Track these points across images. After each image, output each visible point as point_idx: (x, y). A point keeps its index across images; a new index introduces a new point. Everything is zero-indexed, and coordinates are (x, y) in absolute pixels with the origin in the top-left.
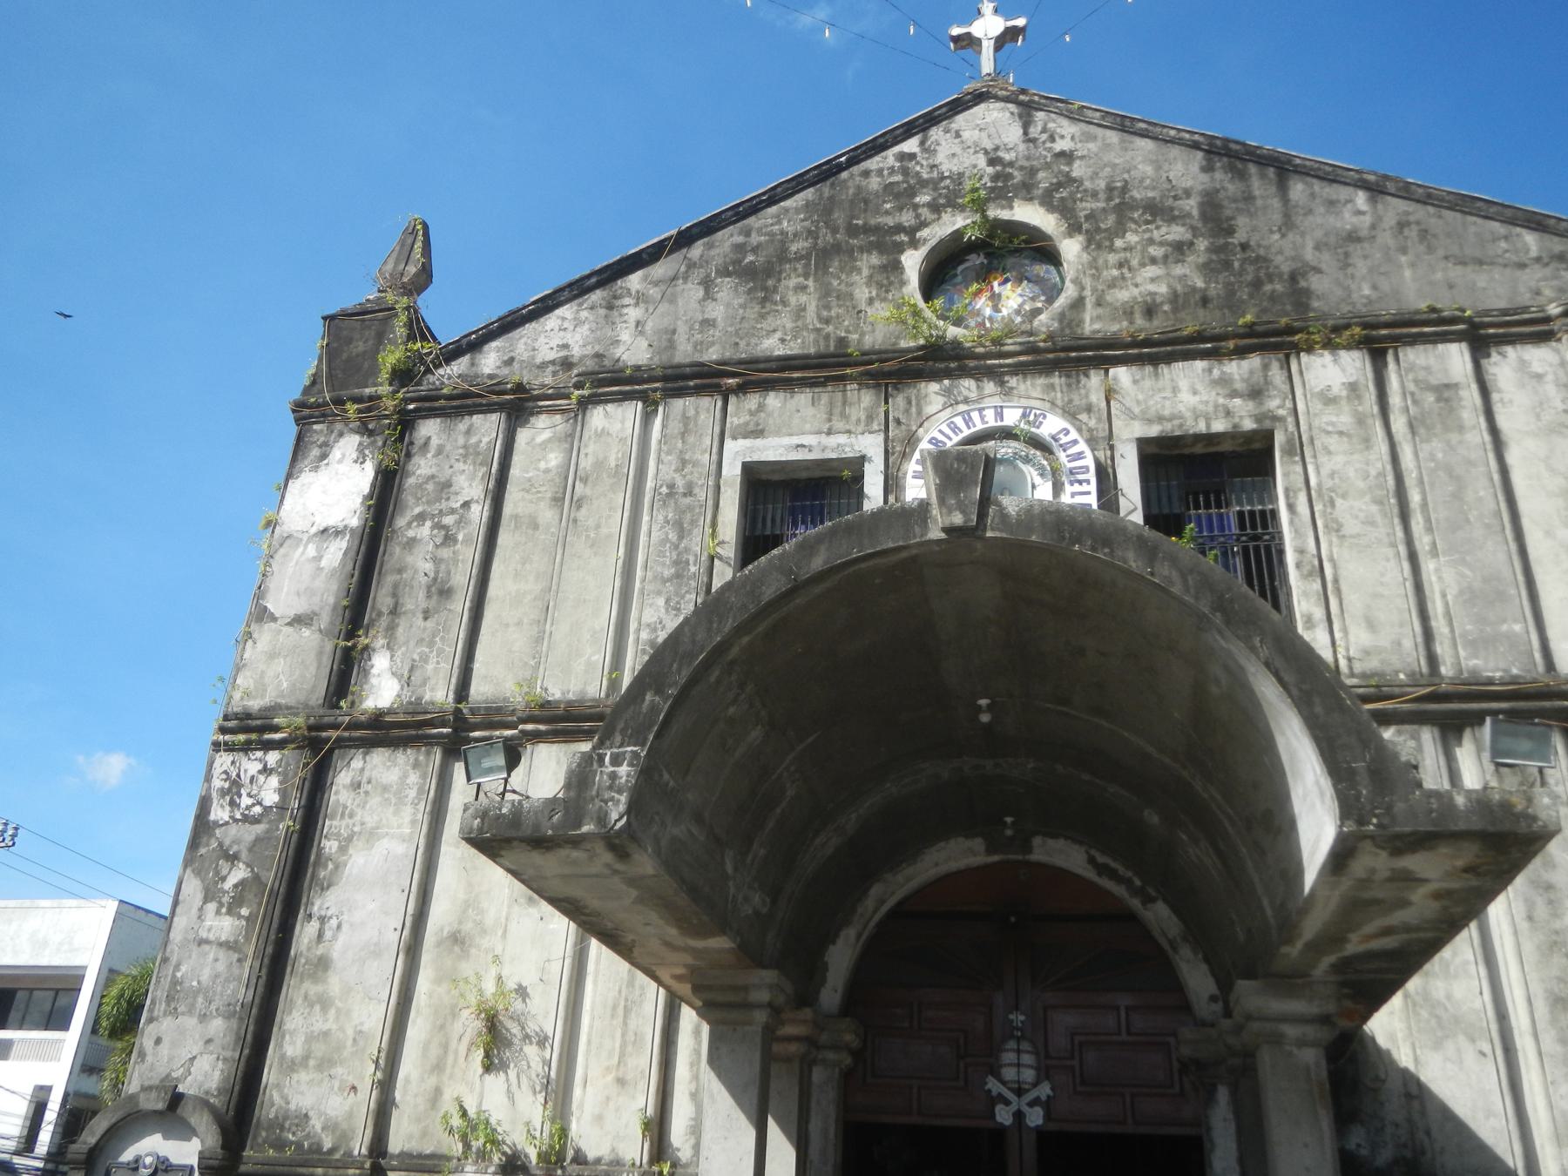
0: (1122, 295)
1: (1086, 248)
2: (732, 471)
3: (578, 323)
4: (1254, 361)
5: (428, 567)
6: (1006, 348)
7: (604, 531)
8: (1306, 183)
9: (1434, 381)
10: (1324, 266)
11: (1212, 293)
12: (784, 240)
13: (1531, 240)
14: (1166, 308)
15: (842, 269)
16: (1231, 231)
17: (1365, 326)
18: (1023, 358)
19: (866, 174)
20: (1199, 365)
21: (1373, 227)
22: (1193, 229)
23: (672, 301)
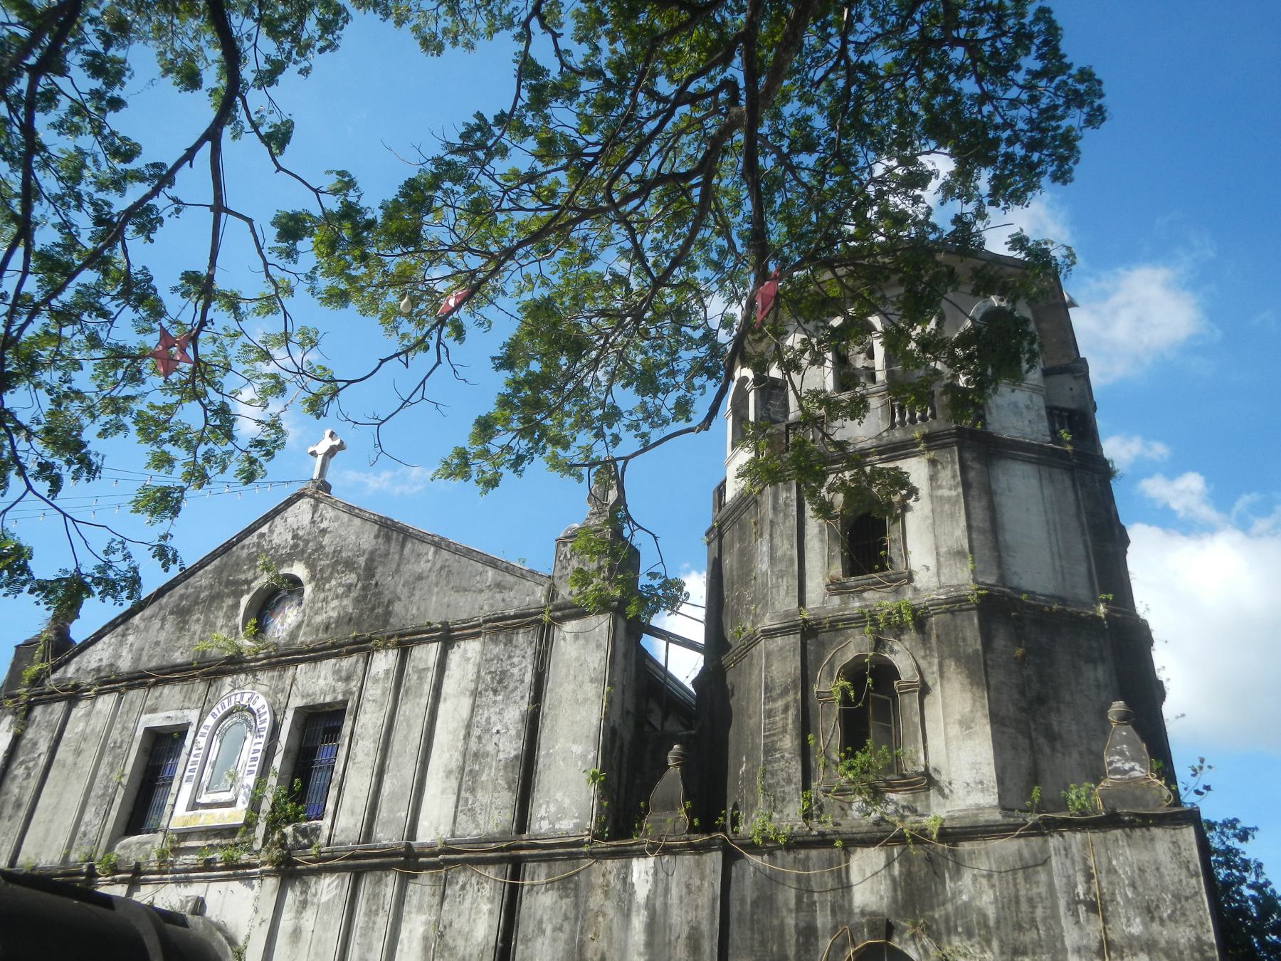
0: (318, 619)
1: (314, 590)
2: (140, 733)
3: (110, 645)
4: (355, 657)
5: (16, 791)
6: (259, 656)
7: (84, 769)
8: (413, 544)
9: (422, 666)
10: (402, 597)
11: (354, 615)
12: (200, 590)
13: (490, 573)
14: (333, 626)
15: (216, 608)
16: (373, 576)
17: (401, 636)
18: (264, 662)
19: (243, 547)
20: (333, 661)
21: (430, 570)
22: (359, 576)
23: (147, 631)
